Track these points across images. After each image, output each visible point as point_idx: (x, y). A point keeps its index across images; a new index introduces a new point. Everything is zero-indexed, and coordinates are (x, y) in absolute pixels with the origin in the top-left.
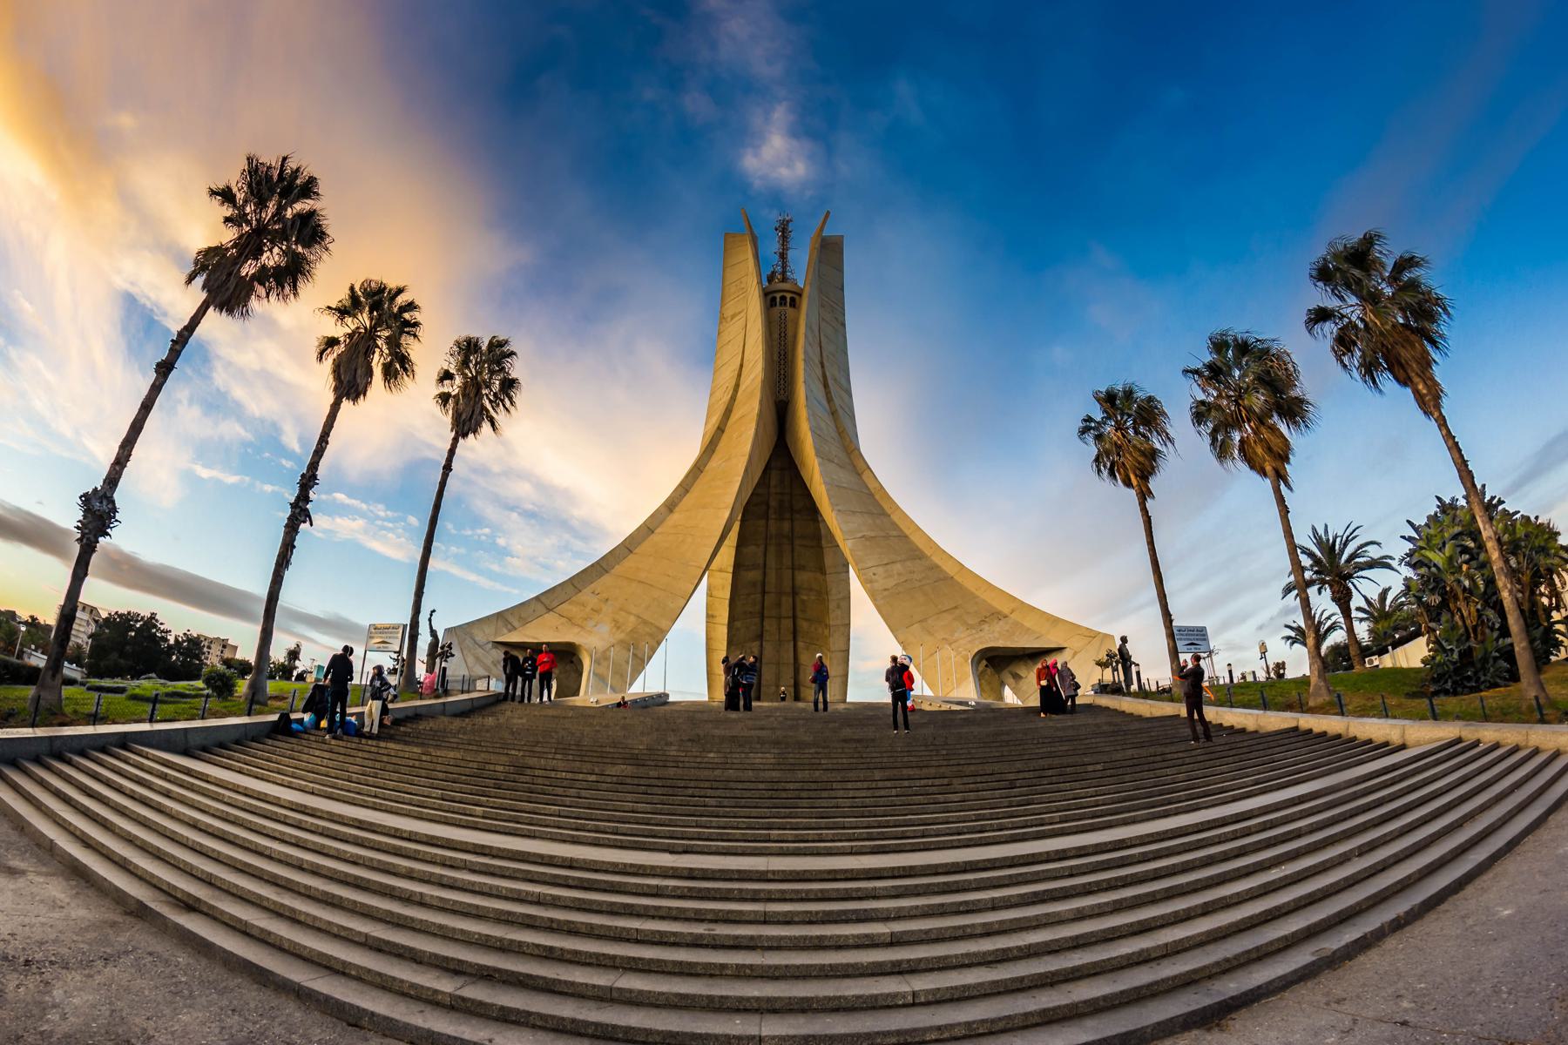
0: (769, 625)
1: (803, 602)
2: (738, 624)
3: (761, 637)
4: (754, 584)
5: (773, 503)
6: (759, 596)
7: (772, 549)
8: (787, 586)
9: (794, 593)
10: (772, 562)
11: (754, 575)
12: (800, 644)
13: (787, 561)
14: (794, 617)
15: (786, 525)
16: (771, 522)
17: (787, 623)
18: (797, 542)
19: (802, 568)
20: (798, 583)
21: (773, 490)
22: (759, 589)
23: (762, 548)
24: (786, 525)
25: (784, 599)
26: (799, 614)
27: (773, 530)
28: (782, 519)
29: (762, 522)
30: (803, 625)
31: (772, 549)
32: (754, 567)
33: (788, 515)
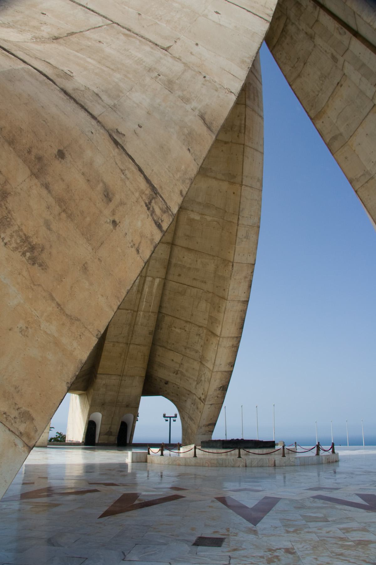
1: (191, 221)
26: (181, 242)
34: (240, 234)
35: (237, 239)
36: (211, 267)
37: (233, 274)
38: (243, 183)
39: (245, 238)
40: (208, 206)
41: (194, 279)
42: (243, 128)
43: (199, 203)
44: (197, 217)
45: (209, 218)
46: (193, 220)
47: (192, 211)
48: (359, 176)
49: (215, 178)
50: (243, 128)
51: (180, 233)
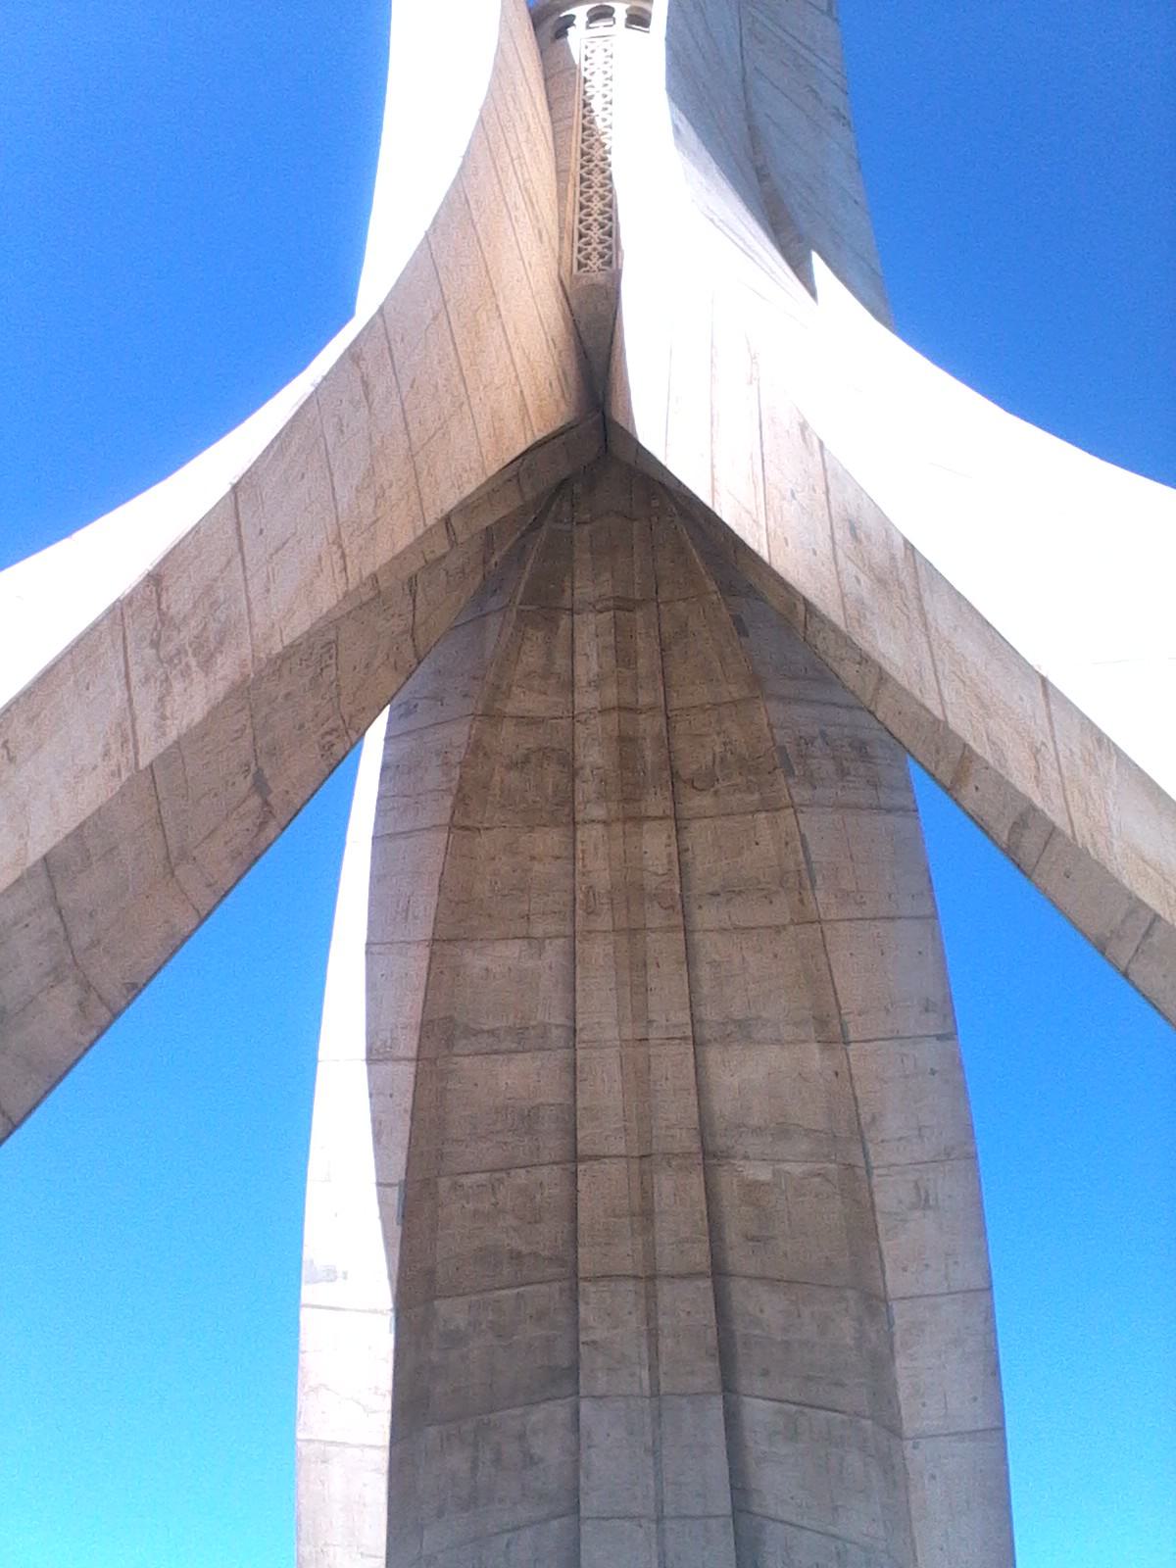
0: (608, 1318)
2: (453, 1312)
3: (564, 1377)
4: (528, 1120)
5: (593, 756)
6: (550, 1176)
7: (598, 952)
8: (675, 1114)
9: (710, 1157)
10: (601, 1009)
11: (520, 1076)
12: (757, 1411)
13: (668, 1007)
14: (718, 1272)
15: (656, 845)
16: (589, 836)
17: (686, 1305)
18: (707, 916)
19: (742, 1031)
20: (723, 1104)
21: (587, 700)
22: (553, 1145)
23: (554, 952)
24: (656, 845)
25: (665, 1184)
26: (738, 1258)
27: (600, 873)
28: (639, 819)
29: (549, 840)
30: (762, 1308)
31: (598, 952)
32: (525, 1038)
33: (655, 803)
34: (884, 1199)
35: (878, 1216)
36: (845, 1328)
37: (897, 1340)
38: (852, 1036)
39: (914, 1207)
40: (783, 1131)
41: (809, 1378)
42: (805, 874)
43: (758, 1131)
44: (764, 1174)
45: (797, 1169)
46: (756, 1185)
47: (746, 1157)
48: (1119, 917)
49: (778, 1041)
50: (805, 874)
51: (732, 1235)
